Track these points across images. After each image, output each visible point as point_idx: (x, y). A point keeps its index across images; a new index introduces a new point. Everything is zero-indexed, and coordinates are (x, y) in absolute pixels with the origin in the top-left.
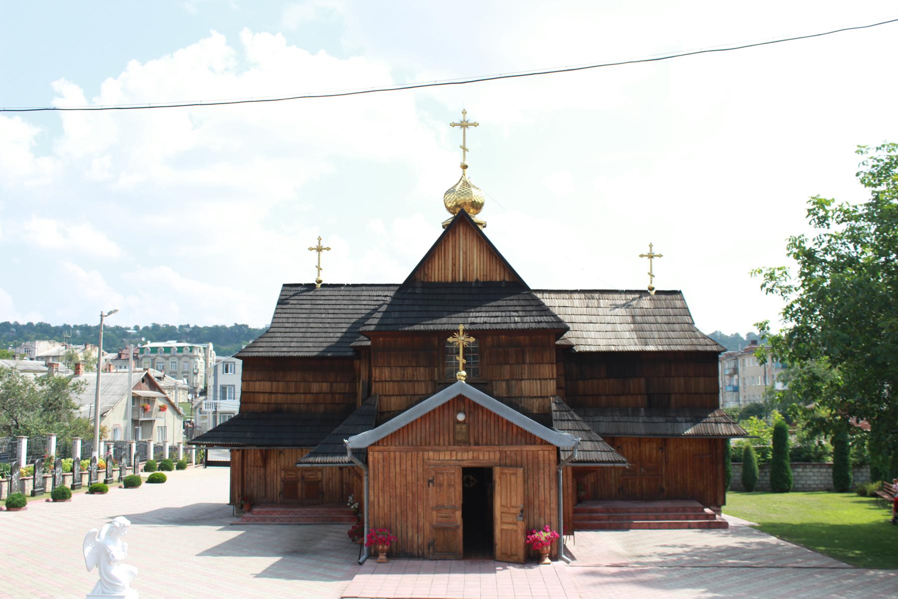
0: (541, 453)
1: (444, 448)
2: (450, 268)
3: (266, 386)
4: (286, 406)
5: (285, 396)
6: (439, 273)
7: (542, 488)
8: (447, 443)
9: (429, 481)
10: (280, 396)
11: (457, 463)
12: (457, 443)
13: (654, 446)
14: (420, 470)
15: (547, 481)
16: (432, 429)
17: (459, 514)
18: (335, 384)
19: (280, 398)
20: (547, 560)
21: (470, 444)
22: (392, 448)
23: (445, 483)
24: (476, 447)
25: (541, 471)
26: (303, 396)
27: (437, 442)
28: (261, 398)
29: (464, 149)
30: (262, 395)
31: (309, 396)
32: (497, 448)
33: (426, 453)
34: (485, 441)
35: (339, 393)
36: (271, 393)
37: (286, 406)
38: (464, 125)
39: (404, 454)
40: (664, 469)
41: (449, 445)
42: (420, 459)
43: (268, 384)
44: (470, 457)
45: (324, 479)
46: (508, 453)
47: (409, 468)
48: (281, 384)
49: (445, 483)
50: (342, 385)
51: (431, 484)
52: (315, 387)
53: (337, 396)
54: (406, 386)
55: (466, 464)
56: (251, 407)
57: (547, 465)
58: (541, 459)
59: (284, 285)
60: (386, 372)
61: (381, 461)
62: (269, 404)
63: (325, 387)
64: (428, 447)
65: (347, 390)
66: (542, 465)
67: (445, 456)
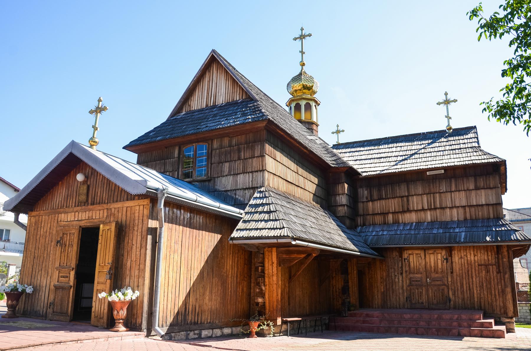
0: (137, 208)
1: (71, 210)
2: (205, 97)
6: (198, 103)
7: (134, 247)
8: (74, 204)
9: (58, 242)
11: (77, 223)
12: (80, 204)
13: (439, 257)
14: (54, 232)
15: (139, 238)
16: (66, 194)
17: (72, 274)
20: (122, 328)
21: (88, 205)
22: (42, 212)
23: (68, 243)
24: (91, 207)
25: (136, 228)
27: (68, 205)
29: (302, 52)
32: (105, 206)
33: (60, 215)
34: (98, 201)
38: (302, 37)
39: (47, 217)
40: (450, 280)
41: (75, 206)
42: (56, 221)
44: (87, 218)
46: (113, 210)
47: (48, 229)
49: (68, 243)
51: (58, 246)
55: (83, 224)
57: (141, 221)
58: (137, 215)
61: (34, 225)
64: (62, 210)
66: (136, 222)
67: (71, 217)
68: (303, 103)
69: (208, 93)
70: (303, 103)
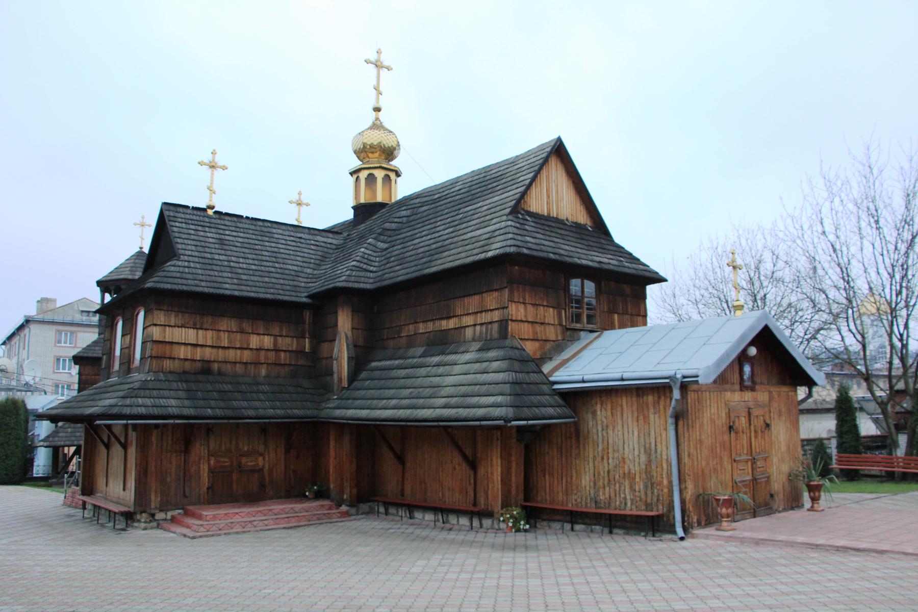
3: (190, 335)
4: (216, 366)
5: (215, 350)
10: (208, 350)
18: (280, 339)
19: (208, 354)
26: (239, 352)
28: (182, 352)
30: (183, 347)
31: (246, 352)
35: (285, 351)
36: (196, 345)
37: (216, 366)
43: (192, 332)
45: (267, 466)
48: (210, 334)
50: (288, 340)
52: (254, 341)
53: (282, 354)
54: (538, 328)
56: (168, 364)
59: (165, 204)
60: (521, 308)
62: (194, 360)
63: (267, 341)
65: (294, 348)
68: (379, 174)
69: (548, 197)
70: (379, 174)
